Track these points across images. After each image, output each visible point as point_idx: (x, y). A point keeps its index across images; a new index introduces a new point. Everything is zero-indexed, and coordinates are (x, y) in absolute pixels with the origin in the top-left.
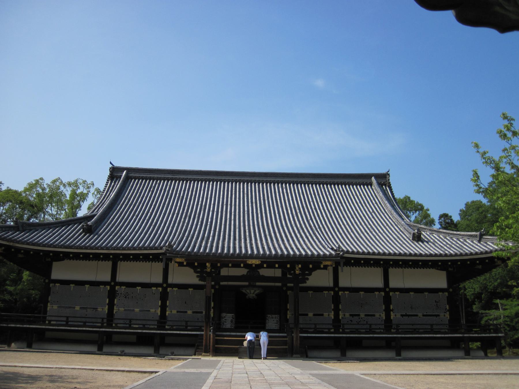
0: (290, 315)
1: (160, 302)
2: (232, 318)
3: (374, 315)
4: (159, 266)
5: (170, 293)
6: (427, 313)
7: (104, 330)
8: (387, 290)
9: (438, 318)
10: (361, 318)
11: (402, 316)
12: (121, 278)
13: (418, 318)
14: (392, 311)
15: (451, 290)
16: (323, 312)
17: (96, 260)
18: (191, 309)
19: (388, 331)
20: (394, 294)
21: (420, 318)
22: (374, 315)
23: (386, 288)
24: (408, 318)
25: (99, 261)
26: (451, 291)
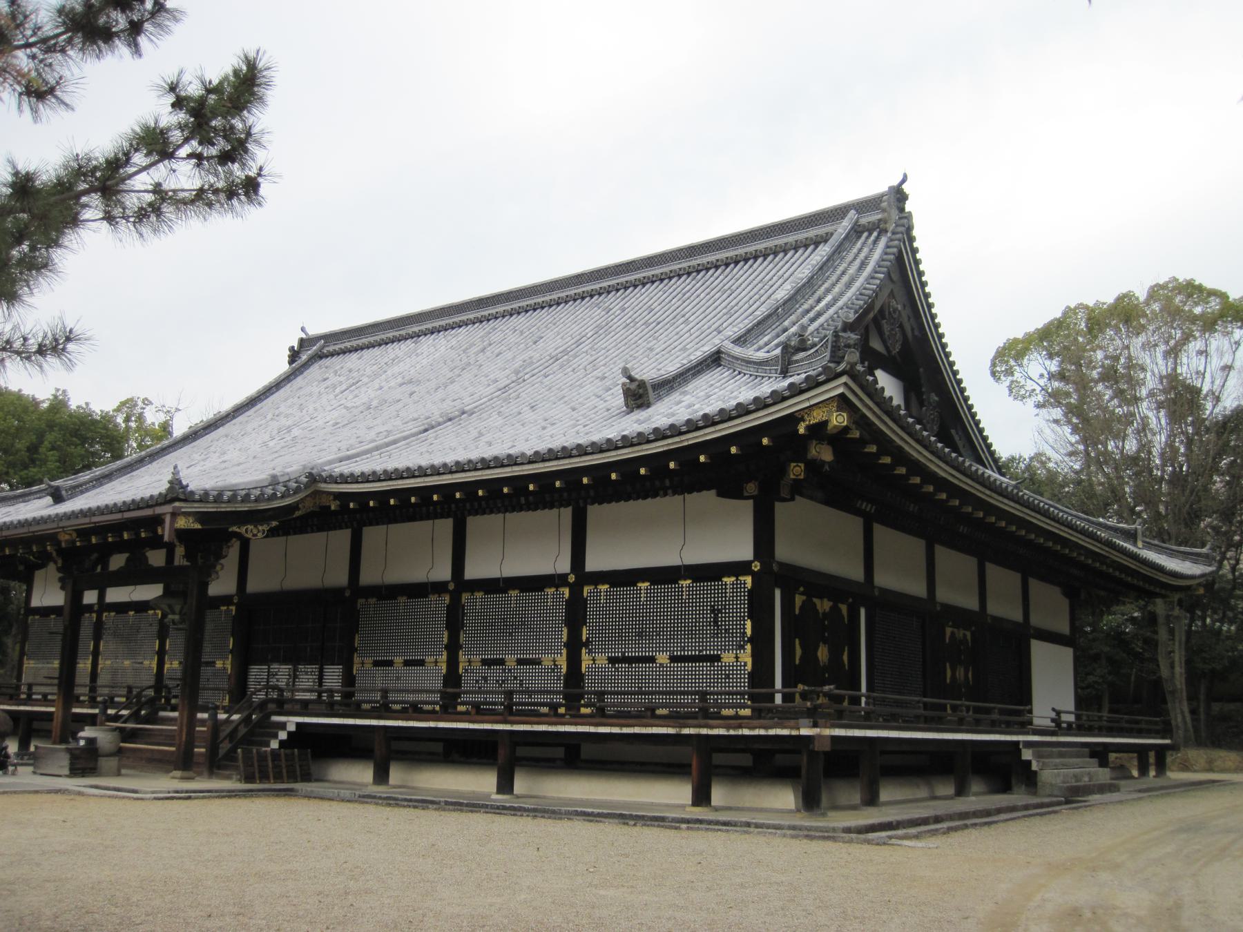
0: (587, 662)
2: (289, 675)
3: (540, 659)
4: (342, 538)
5: (590, 600)
6: (684, 650)
8: (572, 578)
9: (718, 666)
10: (509, 669)
11: (612, 660)
12: (593, 564)
13: (656, 667)
14: (587, 647)
15: (756, 567)
16: (656, 651)
18: (685, 646)
20: (594, 592)
21: (663, 667)
22: (537, 662)
23: (581, 576)
24: (710, 667)
26: (756, 570)
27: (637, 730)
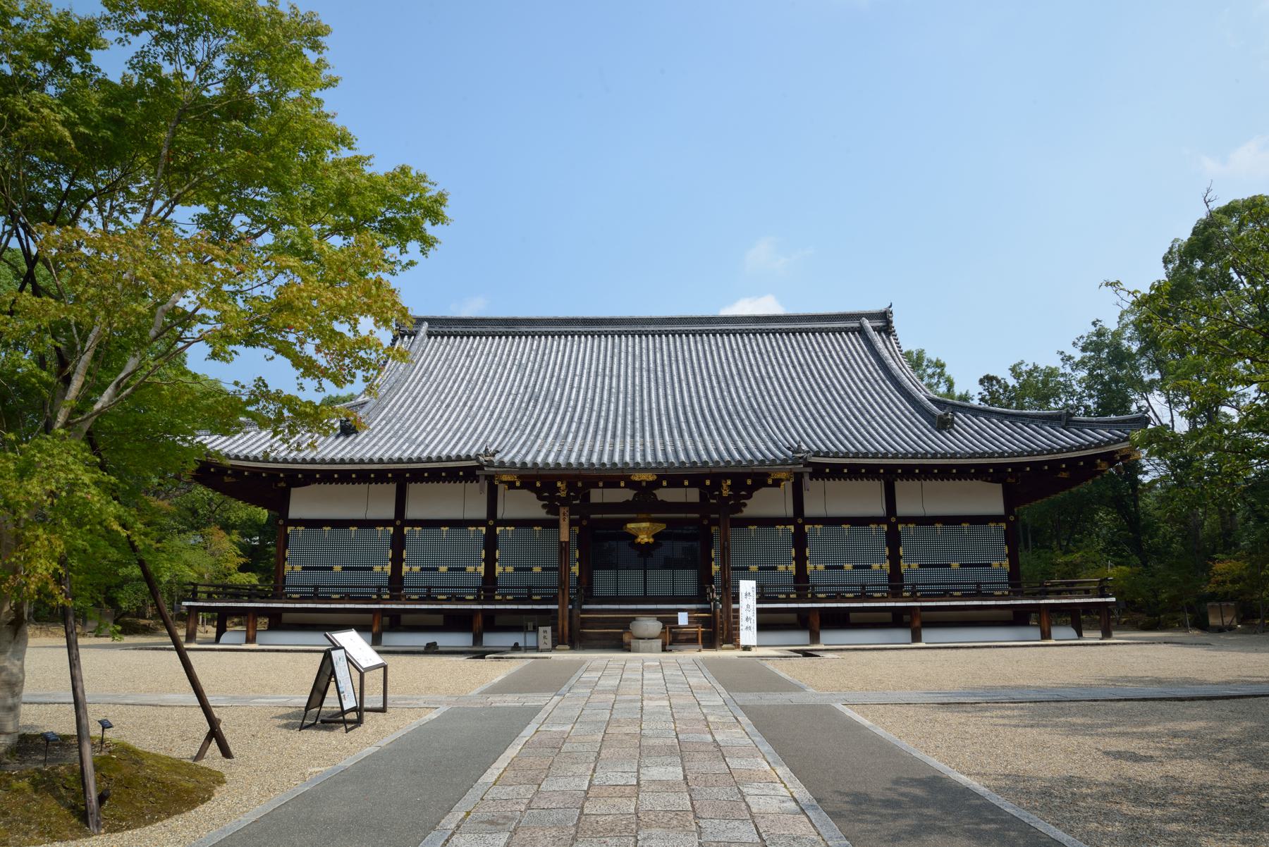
1: (483, 552)
7: (382, 606)
12: (412, 512)
17: (365, 483)
19: (895, 593)
25: (370, 483)
27: (866, 605)
